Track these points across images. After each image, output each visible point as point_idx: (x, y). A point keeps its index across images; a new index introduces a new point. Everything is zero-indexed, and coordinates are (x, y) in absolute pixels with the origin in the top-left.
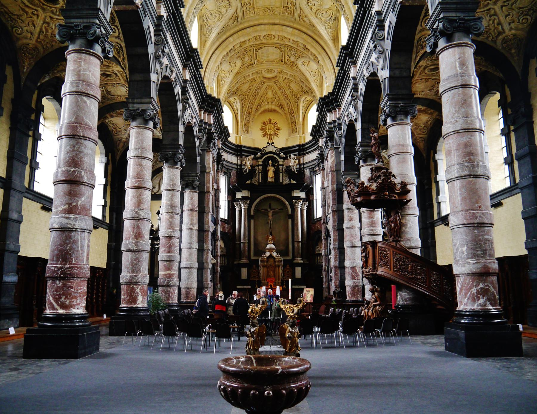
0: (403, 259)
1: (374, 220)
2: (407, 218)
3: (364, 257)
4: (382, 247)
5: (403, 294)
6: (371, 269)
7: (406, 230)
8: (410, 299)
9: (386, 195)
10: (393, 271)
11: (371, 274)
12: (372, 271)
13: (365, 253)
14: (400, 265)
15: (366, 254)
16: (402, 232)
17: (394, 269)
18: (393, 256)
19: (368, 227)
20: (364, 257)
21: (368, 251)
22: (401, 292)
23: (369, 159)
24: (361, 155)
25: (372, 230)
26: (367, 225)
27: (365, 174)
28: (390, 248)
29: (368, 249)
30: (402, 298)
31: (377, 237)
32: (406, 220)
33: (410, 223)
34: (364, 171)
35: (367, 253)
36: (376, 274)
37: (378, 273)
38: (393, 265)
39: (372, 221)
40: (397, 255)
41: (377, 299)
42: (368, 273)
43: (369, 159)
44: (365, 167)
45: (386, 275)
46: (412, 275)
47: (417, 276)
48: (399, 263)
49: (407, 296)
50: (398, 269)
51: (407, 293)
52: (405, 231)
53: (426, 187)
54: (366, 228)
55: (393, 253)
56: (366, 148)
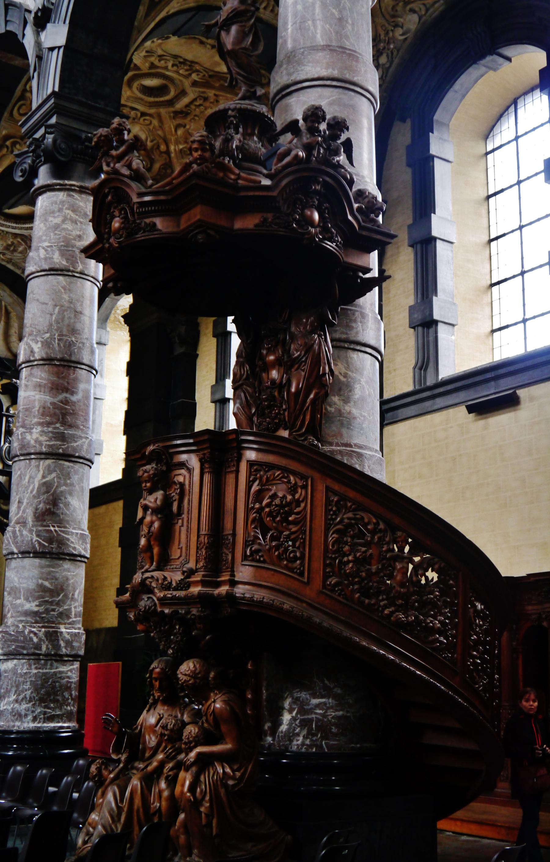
0: (373, 532)
1: (74, 398)
2: (355, 356)
3: (155, 511)
4: (271, 467)
5: (315, 701)
6: (191, 572)
7: (347, 408)
8: (341, 722)
9: (313, 226)
10: (324, 586)
11: (202, 598)
12: (203, 583)
13: (159, 495)
14: (356, 561)
15: (167, 501)
16: (329, 417)
17: (326, 577)
18: (327, 511)
19: (48, 424)
20: (155, 511)
21: (182, 485)
22: (303, 695)
23: (80, 168)
24: (54, 141)
25: (62, 437)
26: (43, 414)
27: (58, 220)
28: (309, 472)
29: (181, 476)
30: (305, 723)
31: (77, 466)
32: (348, 367)
33: (363, 381)
34: (55, 207)
35: (175, 495)
36: (230, 596)
37: (240, 590)
38: (325, 557)
39: (66, 402)
40: (348, 510)
41: (224, 728)
42: (181, 594)
43: (80, 168)
44: (61, 196)
45: (288, 603)
46: (405, 609)
47: (427, 615)
48: (354, 548)
49: (332, 713)
50: (347, 576)
51: (336, 697)
52: (340, 413)
53: (179, 350)
54: (39, 428)
55: (328, 502)
56: (75, 125)
